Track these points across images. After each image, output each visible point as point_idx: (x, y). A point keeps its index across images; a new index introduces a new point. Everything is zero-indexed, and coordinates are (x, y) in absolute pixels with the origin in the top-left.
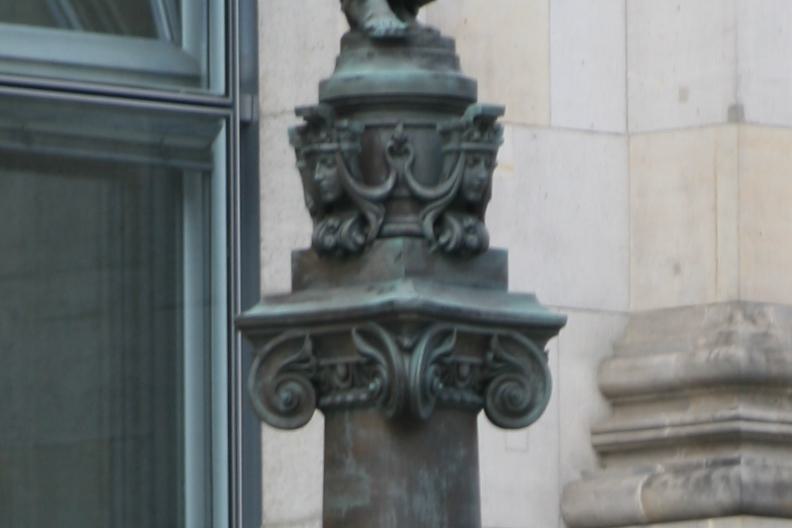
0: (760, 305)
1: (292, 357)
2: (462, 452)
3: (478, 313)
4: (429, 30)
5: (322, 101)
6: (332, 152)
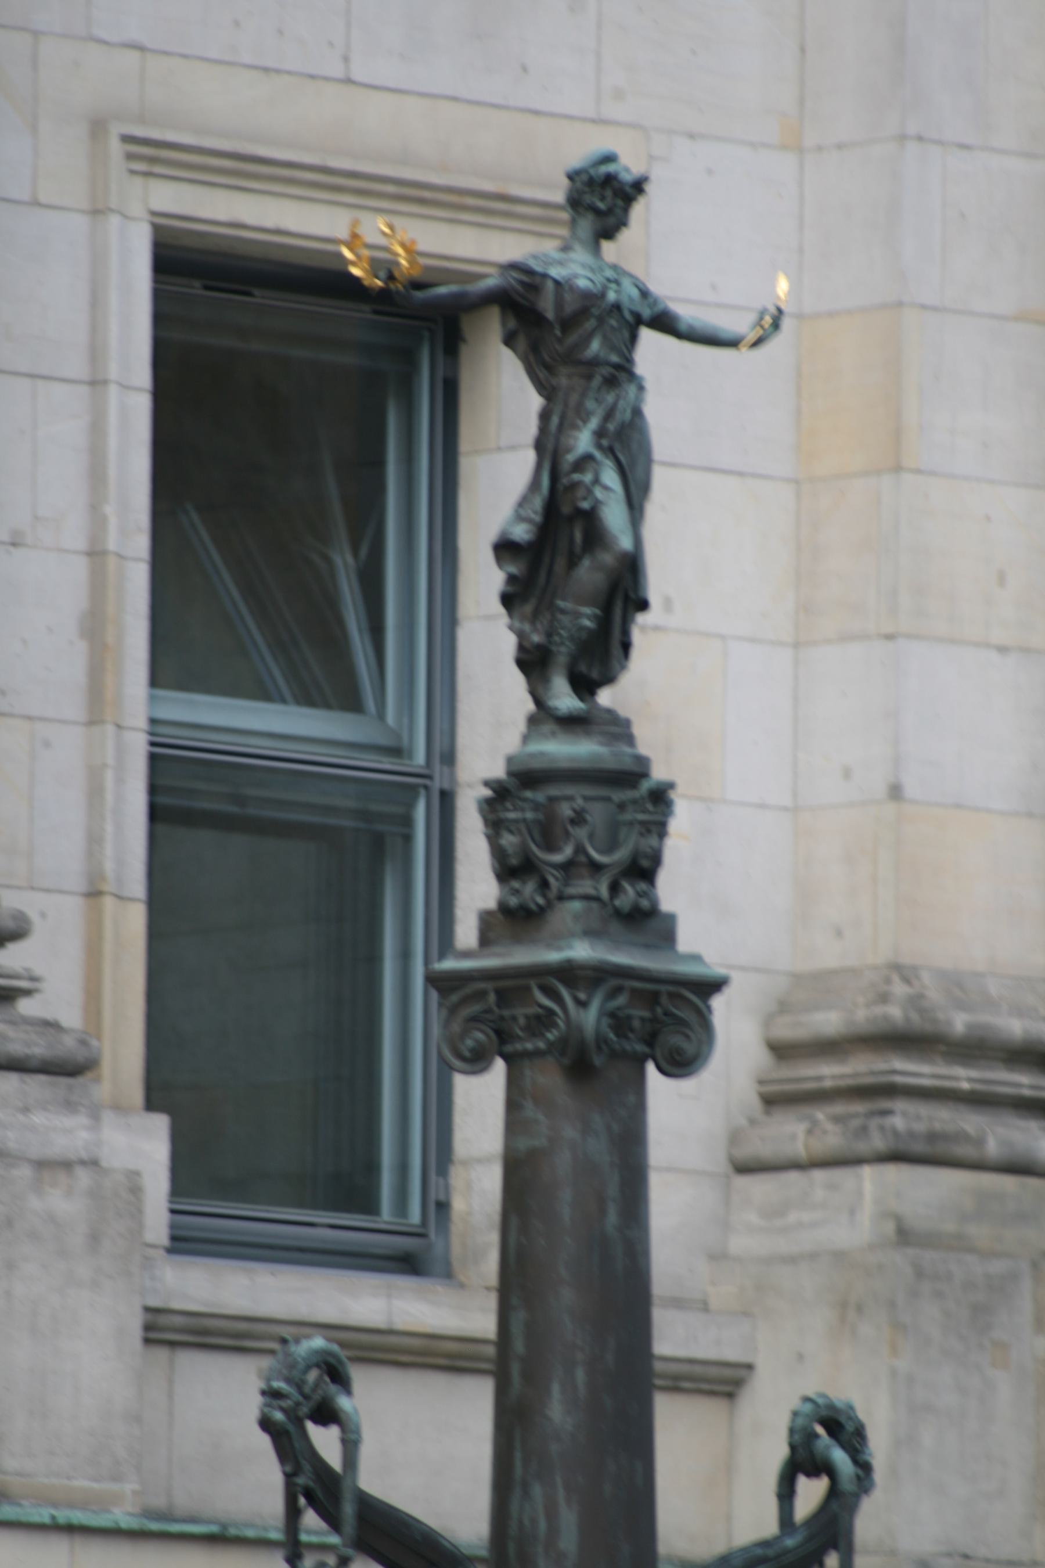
0: (915, 969)
1: (475, 1008)
2: (631, 1099)
3: (648, 970)
4: (609, 711)
5: (510, 773)
6: (516, 821)
